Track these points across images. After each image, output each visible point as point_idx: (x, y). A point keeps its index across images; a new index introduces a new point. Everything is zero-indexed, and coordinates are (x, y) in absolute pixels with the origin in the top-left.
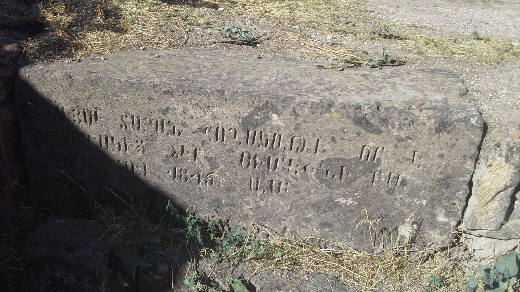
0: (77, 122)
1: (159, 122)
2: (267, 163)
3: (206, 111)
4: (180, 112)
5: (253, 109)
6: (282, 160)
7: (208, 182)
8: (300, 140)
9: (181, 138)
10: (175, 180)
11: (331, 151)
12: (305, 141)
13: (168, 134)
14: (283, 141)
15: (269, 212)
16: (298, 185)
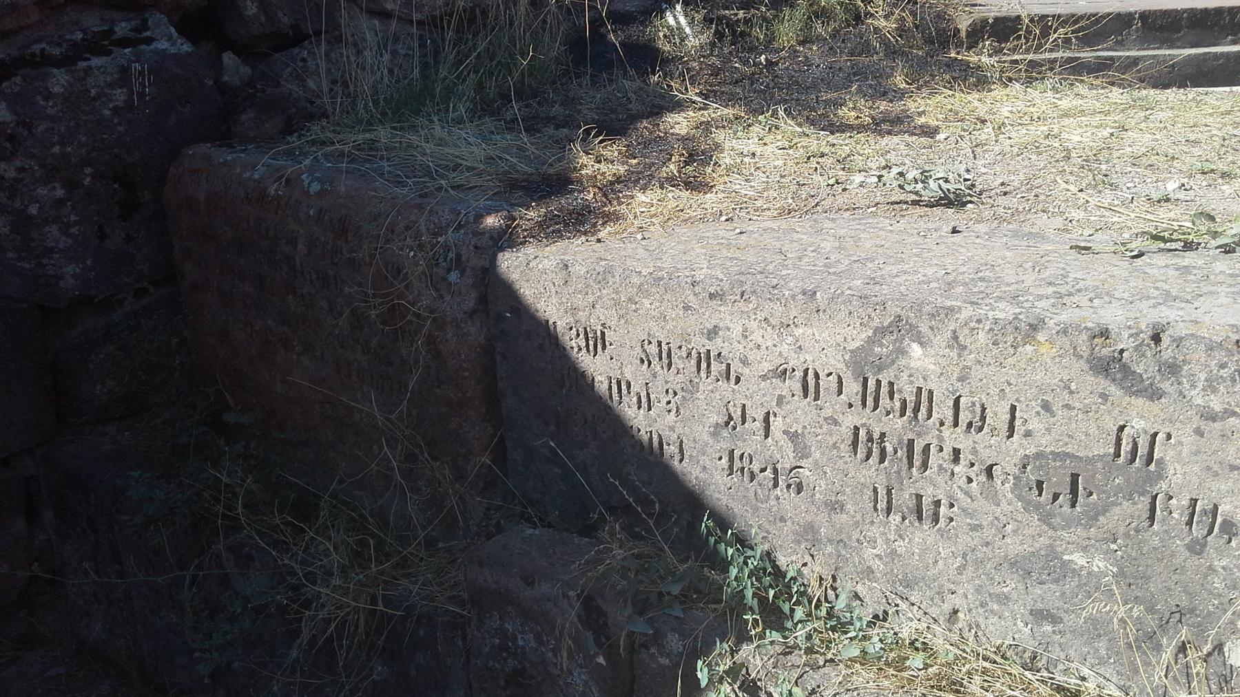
3: (784, 334)
5: (870, 333)
6: (938, 448)
8: (974, 404)
12: (984, 409)
13: (719, 380)
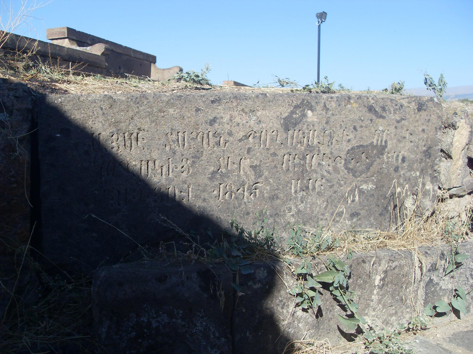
1: (205, 136)
3: (251, 116)
4: (227, 121)
8: (331, 132)
9: (228, 149)
11: (354, 139)
15: (309, 214)
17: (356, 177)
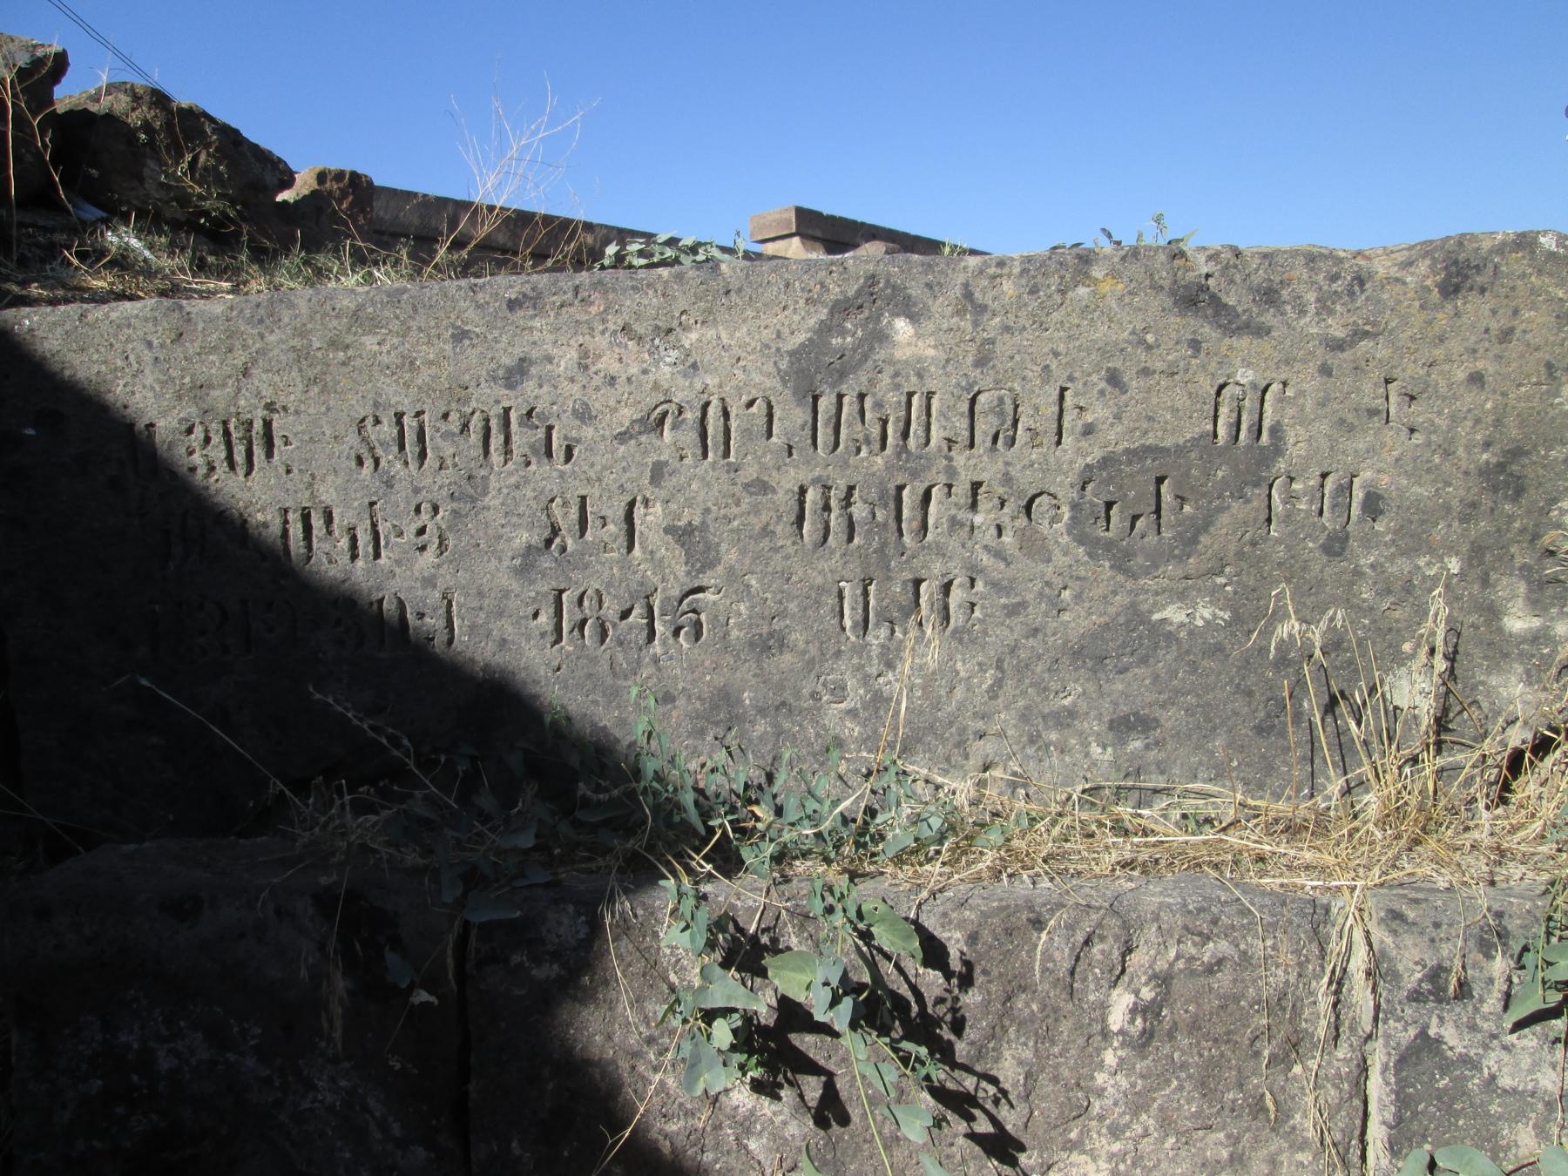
0: (202, 471)
1: (494, 423)
2: (893, 514)
3: (662, 348)
4: (566, 368)
5: (823, 313)
7: (682, 632)
8: (1001, 400)
9: (576, 469)
10: (563, 643)
11: (1112, 425)
13: (528, 464)
14: (942, 414)
15: (921, 713)
16: (1013, 580)
17: (1133, 576)
